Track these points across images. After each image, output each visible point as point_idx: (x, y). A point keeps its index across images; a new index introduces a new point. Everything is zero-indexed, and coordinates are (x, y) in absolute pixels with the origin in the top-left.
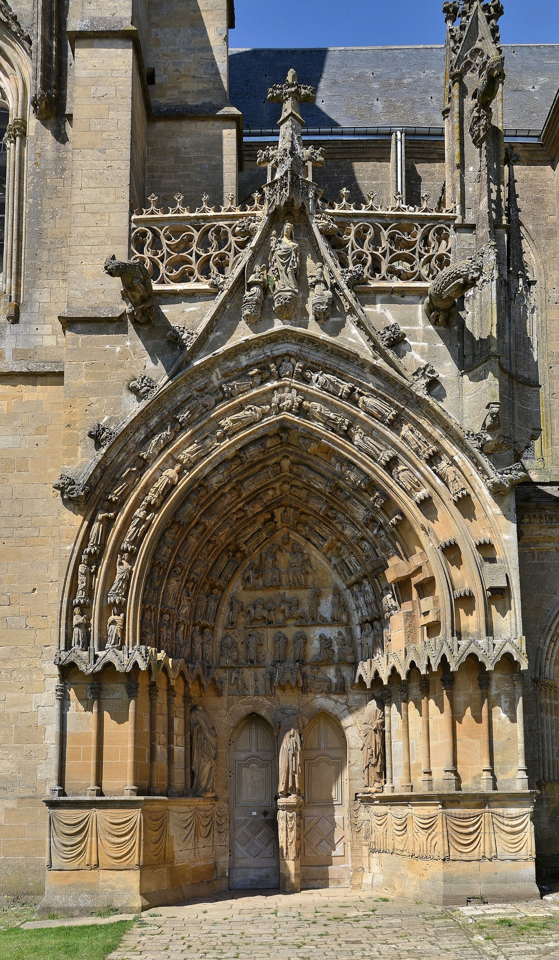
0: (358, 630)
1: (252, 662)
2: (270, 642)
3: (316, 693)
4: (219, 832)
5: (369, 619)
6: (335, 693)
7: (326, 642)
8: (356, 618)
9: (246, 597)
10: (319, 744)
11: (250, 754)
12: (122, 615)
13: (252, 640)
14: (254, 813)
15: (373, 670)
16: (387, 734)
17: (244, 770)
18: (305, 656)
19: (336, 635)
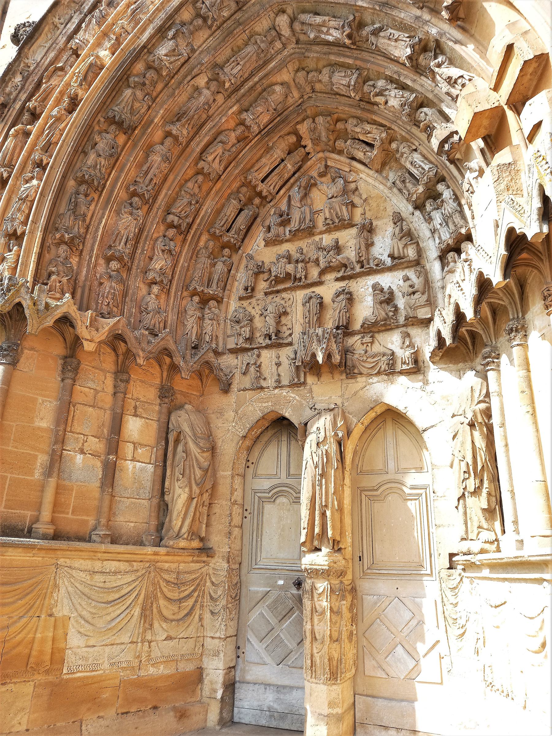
0: (435, 268)
4: (212, 613)
10: (386, 463)
11: (276, 482)
14: (281, 582)
17: (268, 507)
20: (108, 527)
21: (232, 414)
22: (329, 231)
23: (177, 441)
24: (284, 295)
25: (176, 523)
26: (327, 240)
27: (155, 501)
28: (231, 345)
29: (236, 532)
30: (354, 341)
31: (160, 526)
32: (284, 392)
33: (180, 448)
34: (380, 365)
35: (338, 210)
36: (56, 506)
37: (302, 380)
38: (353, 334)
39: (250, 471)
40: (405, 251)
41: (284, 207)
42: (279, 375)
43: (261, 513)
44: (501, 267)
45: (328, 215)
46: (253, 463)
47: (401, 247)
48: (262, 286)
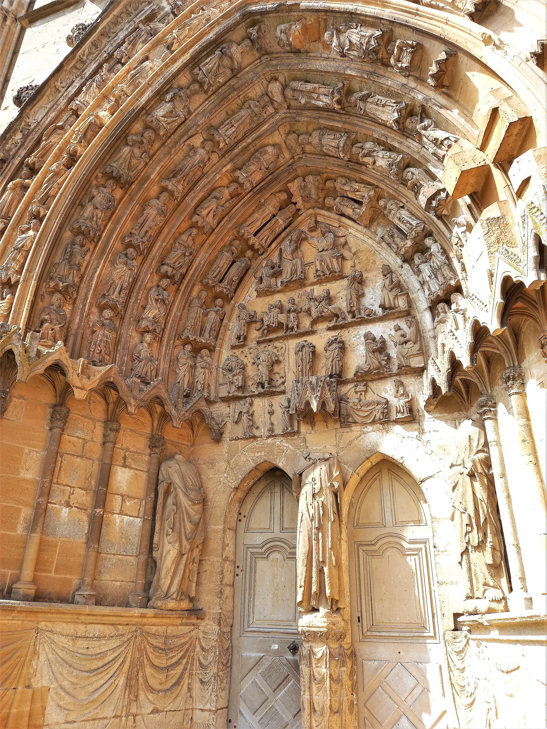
0: (427, 317)
4: (202, 682)
11: (269, 536)
14: (276, 647)
17: (261, 564)
20: (93, 586)
21: (224, 464)
22: (320, 282)
23: (167, 493)
24: (277, 344)
25: (165, 582)
26: (318, 291)
27: (143, 557)
28: (223, 393)
29: (228, 591)
30: (348, 389)
31: (148, 586)
32: (278, 442)
33: (170, 500)
34: (374, 413)
35: (329, 262)
36: (39, 564)
37: (296, 429)
38: (346, 382)
39: (242, 524)
40: (396, 301)
41: (275, 259)
42: (272, 424)
43: (253, 569)
44: (498, 315)
45: (319, 268)
46: (245, 516)
48: (255, 335)
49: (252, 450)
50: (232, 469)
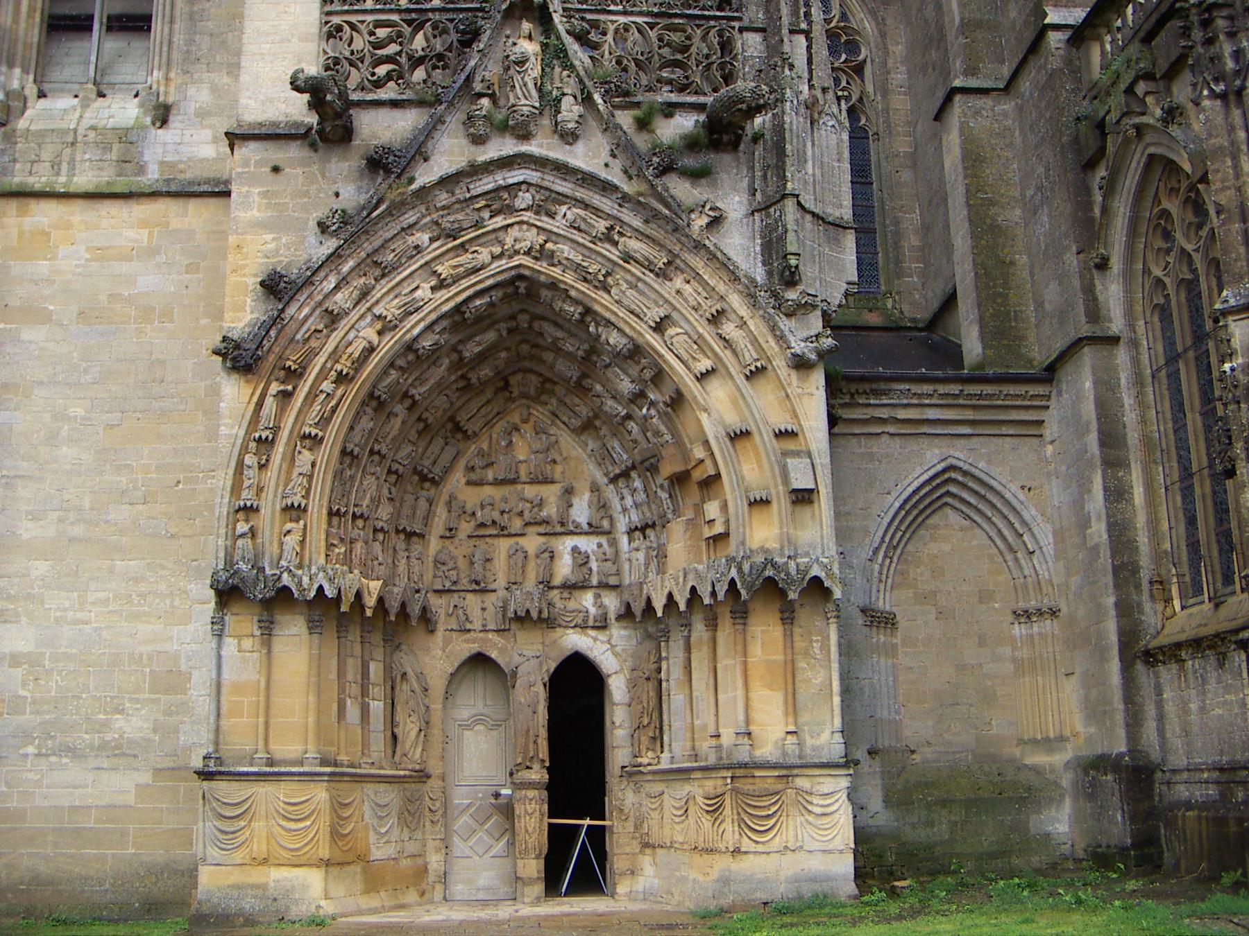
1: (477, 583)
2: (503, 556)
3: (566, 627)
4: (432, 822)
5: (639, 526)
6: (593, 628)
7: (581, 560)
8: (622, 525)
9: (471, 497)
11: (474, 711)
12: (302, 522)
13: (478, 557)
15: (644, 596)
16: (664, 684)
17: (466, 733)
18: (551, 575)
19: (595, 547)
24: (488, 539)
26: (530, 491)
32: (490, 635)
38: (553, 588)
47: (598, 518)
49: (467, 641)
50: (447, 657)
